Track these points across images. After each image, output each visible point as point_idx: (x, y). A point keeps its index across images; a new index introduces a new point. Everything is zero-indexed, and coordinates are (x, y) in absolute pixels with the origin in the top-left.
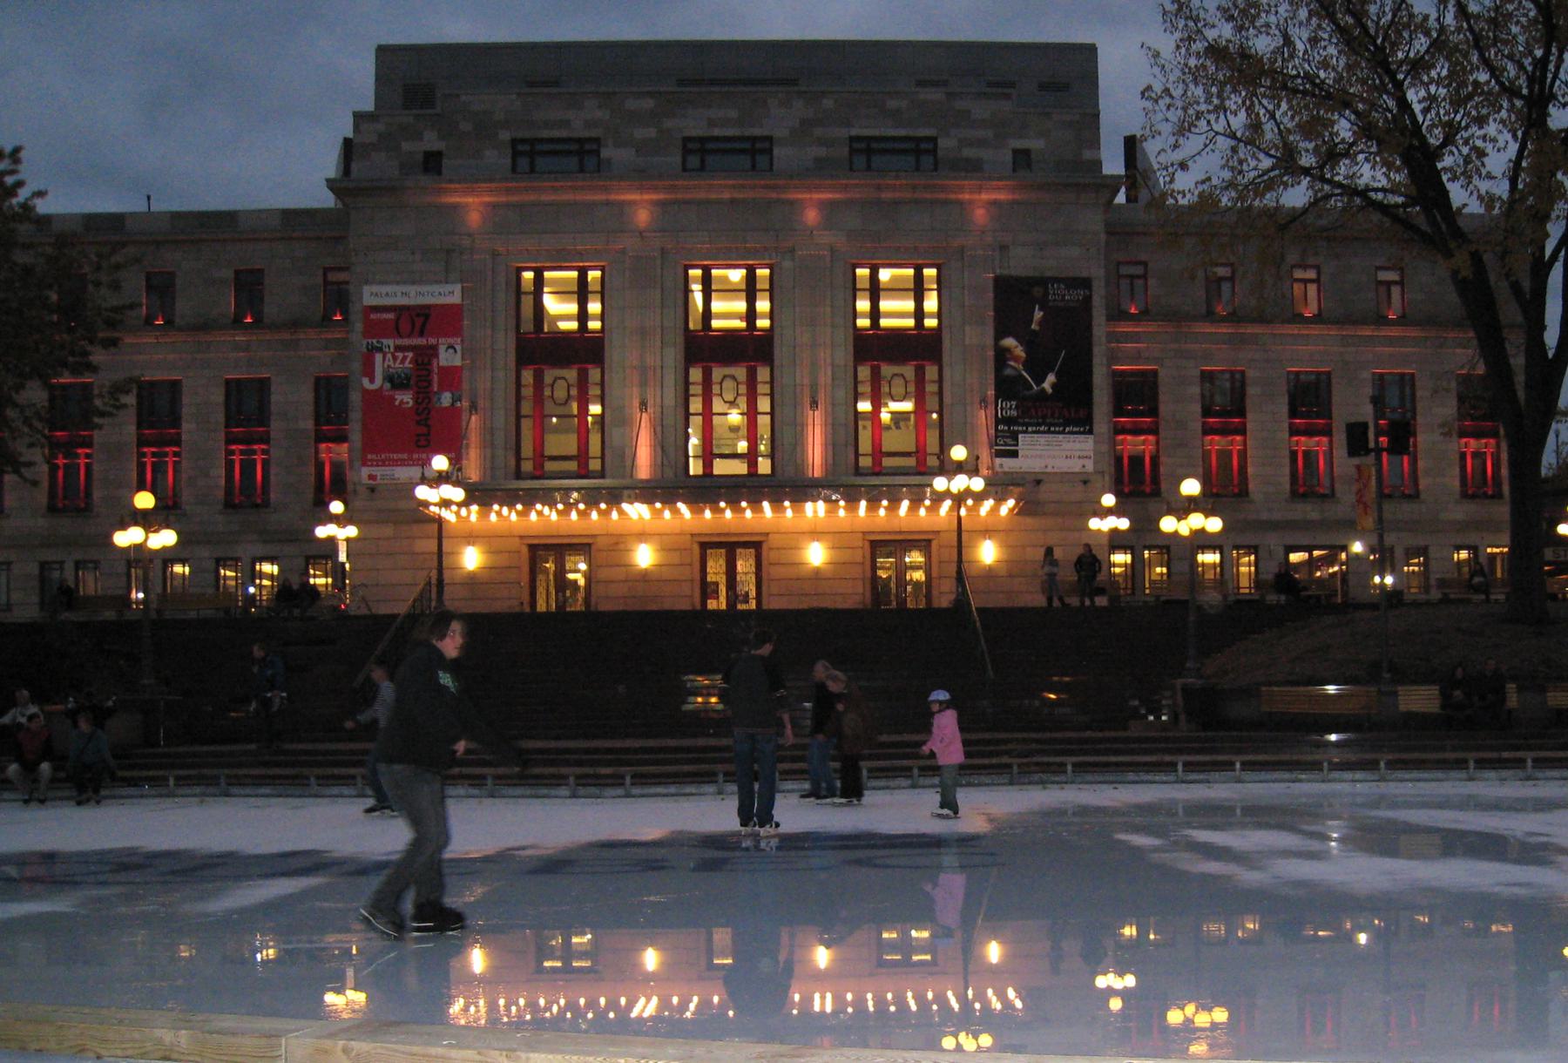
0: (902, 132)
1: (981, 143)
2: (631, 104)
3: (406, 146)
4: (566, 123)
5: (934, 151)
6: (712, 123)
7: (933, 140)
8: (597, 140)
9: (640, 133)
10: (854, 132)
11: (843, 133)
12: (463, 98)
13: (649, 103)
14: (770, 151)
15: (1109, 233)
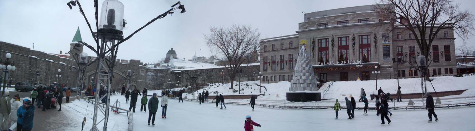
9: (332, 21)
11: (357, 19)
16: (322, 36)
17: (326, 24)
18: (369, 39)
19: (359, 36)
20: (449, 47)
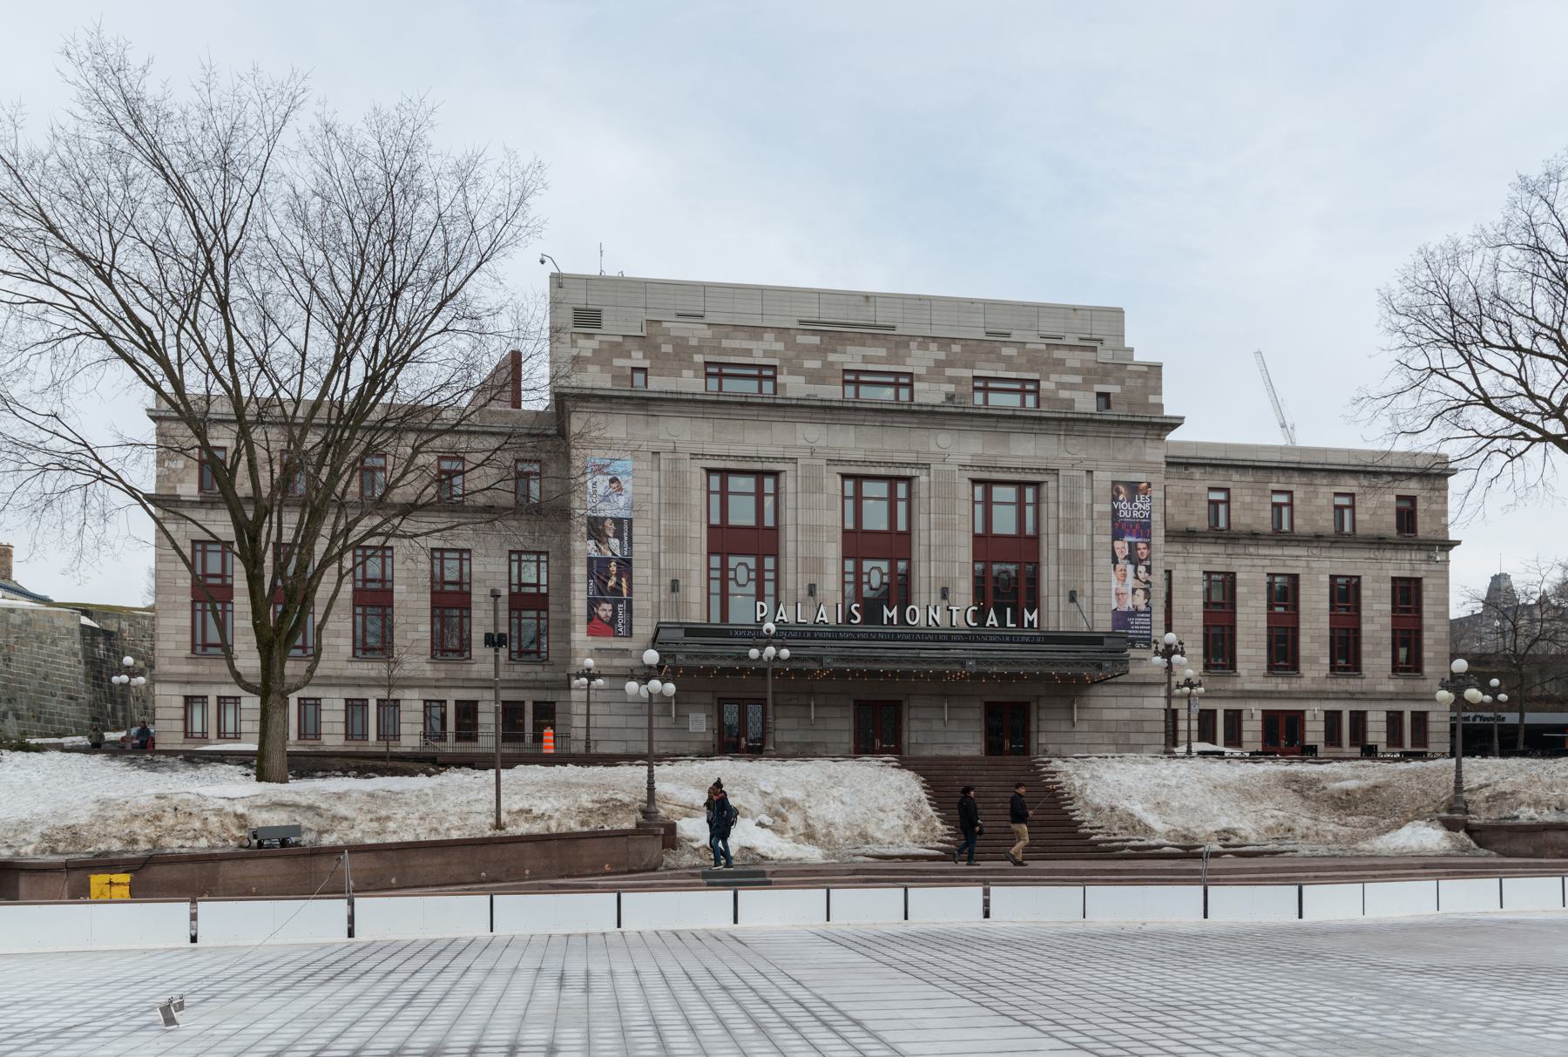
0: (1013, 375)
1: (1072, 387)
3: (618, 362)
4: (749, 352)
5: (1036, 392)
6: (865, 359)
7: (1038, 381)
8: (774, 367)
9: (812, 364)
10: (977, 373)
11: (968, 373)
12: (665, 325)
13: (816, 340)
14: (910, 385)
15: (1169, 464)
17: (766, 373)
19: (975, 482)
20: (1358, 587)
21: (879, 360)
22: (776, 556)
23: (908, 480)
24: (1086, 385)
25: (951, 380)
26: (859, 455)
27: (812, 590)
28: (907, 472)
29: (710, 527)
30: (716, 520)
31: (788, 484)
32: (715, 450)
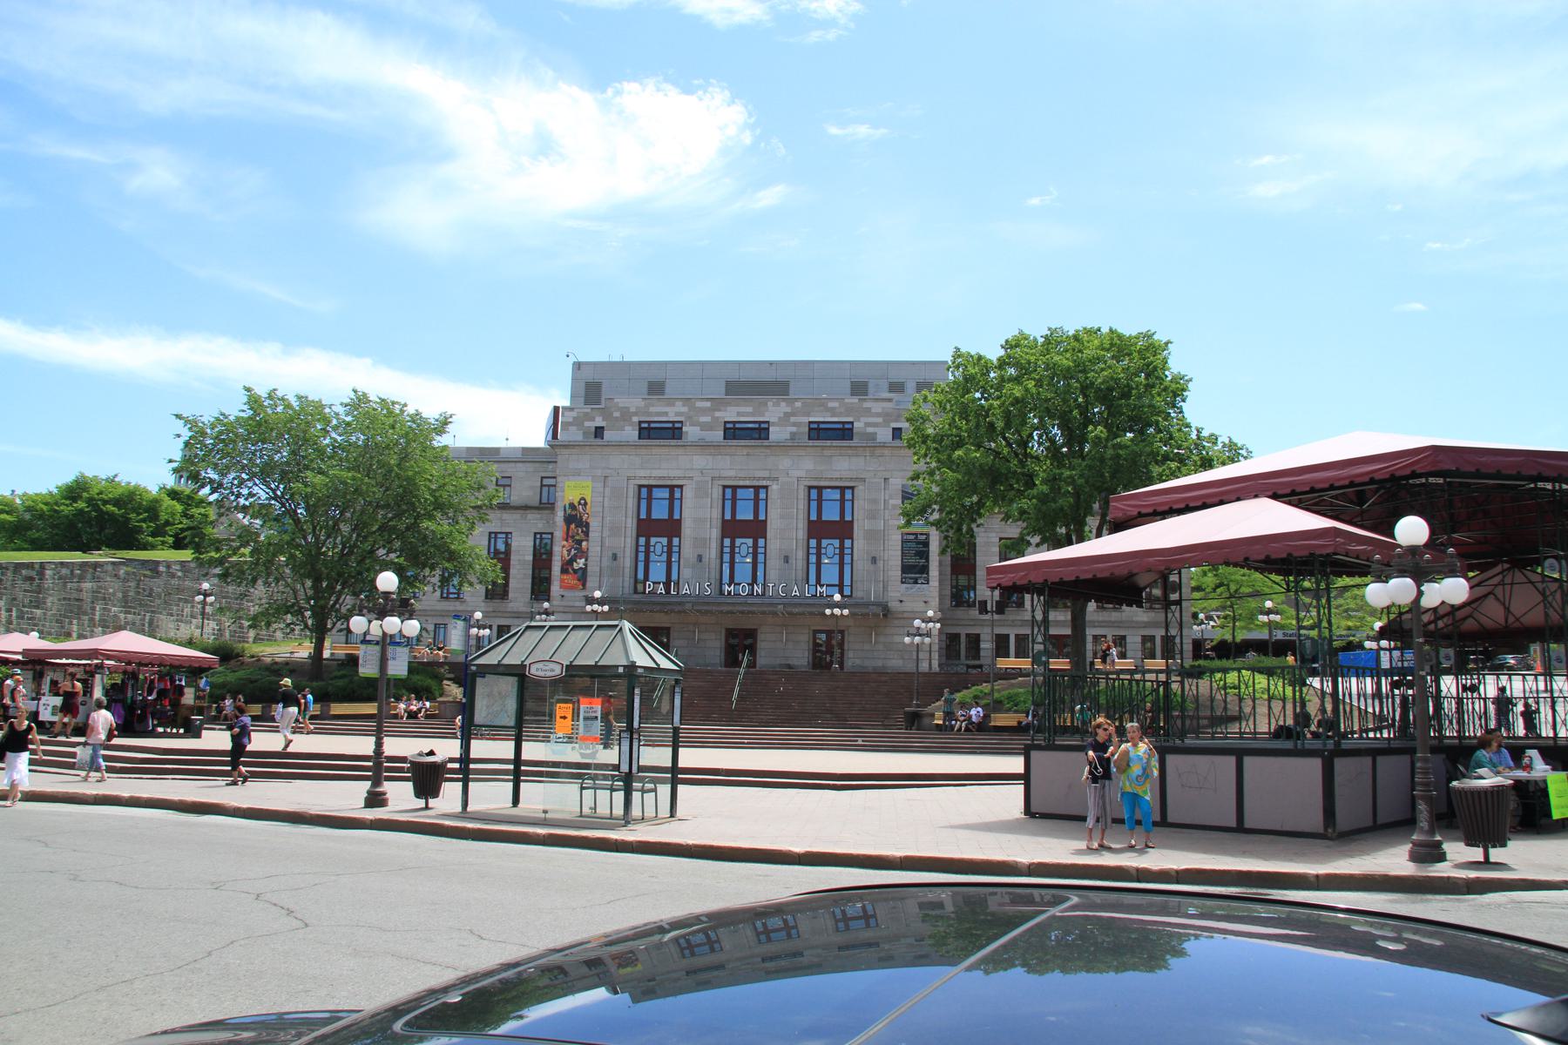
2: (699, 404)
3: (587, 424)
4: (666, 414)
6: (739, 414)
11: (806, 420)
13: (708, 404)
16: (656, 473)
18: (848, 505)
21: (748, 414)
22: (679, 536)
23: (766, 487)
24: (886, 423)
25: (794, 424)
26: (732, 473)
27: (700, 558)
28: (764, 483)
29: (639, 520)
30: (643, 516)
31: (688, 493)
32: (642, 473)
